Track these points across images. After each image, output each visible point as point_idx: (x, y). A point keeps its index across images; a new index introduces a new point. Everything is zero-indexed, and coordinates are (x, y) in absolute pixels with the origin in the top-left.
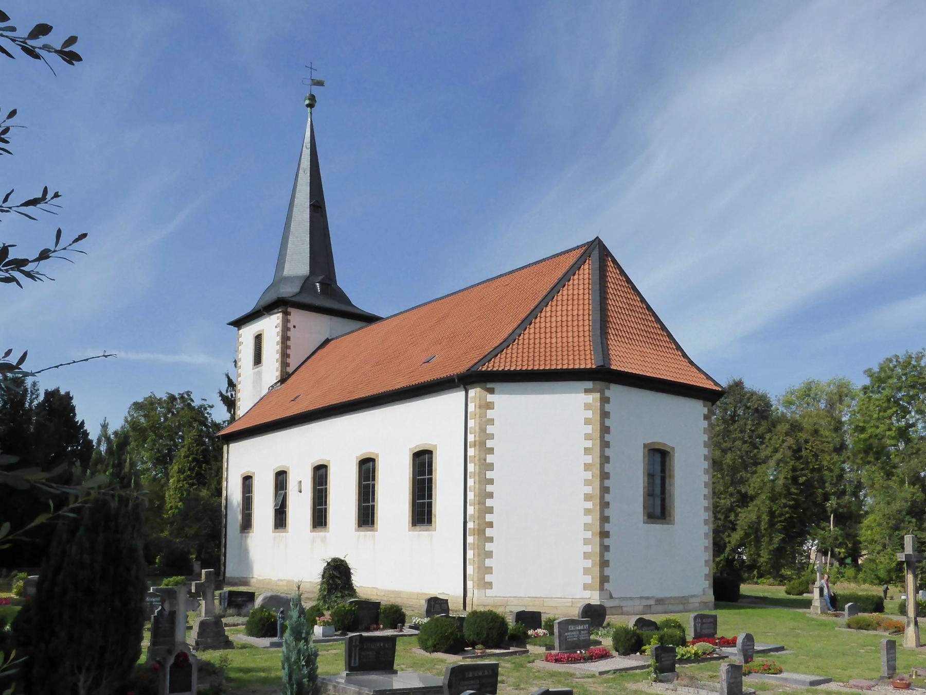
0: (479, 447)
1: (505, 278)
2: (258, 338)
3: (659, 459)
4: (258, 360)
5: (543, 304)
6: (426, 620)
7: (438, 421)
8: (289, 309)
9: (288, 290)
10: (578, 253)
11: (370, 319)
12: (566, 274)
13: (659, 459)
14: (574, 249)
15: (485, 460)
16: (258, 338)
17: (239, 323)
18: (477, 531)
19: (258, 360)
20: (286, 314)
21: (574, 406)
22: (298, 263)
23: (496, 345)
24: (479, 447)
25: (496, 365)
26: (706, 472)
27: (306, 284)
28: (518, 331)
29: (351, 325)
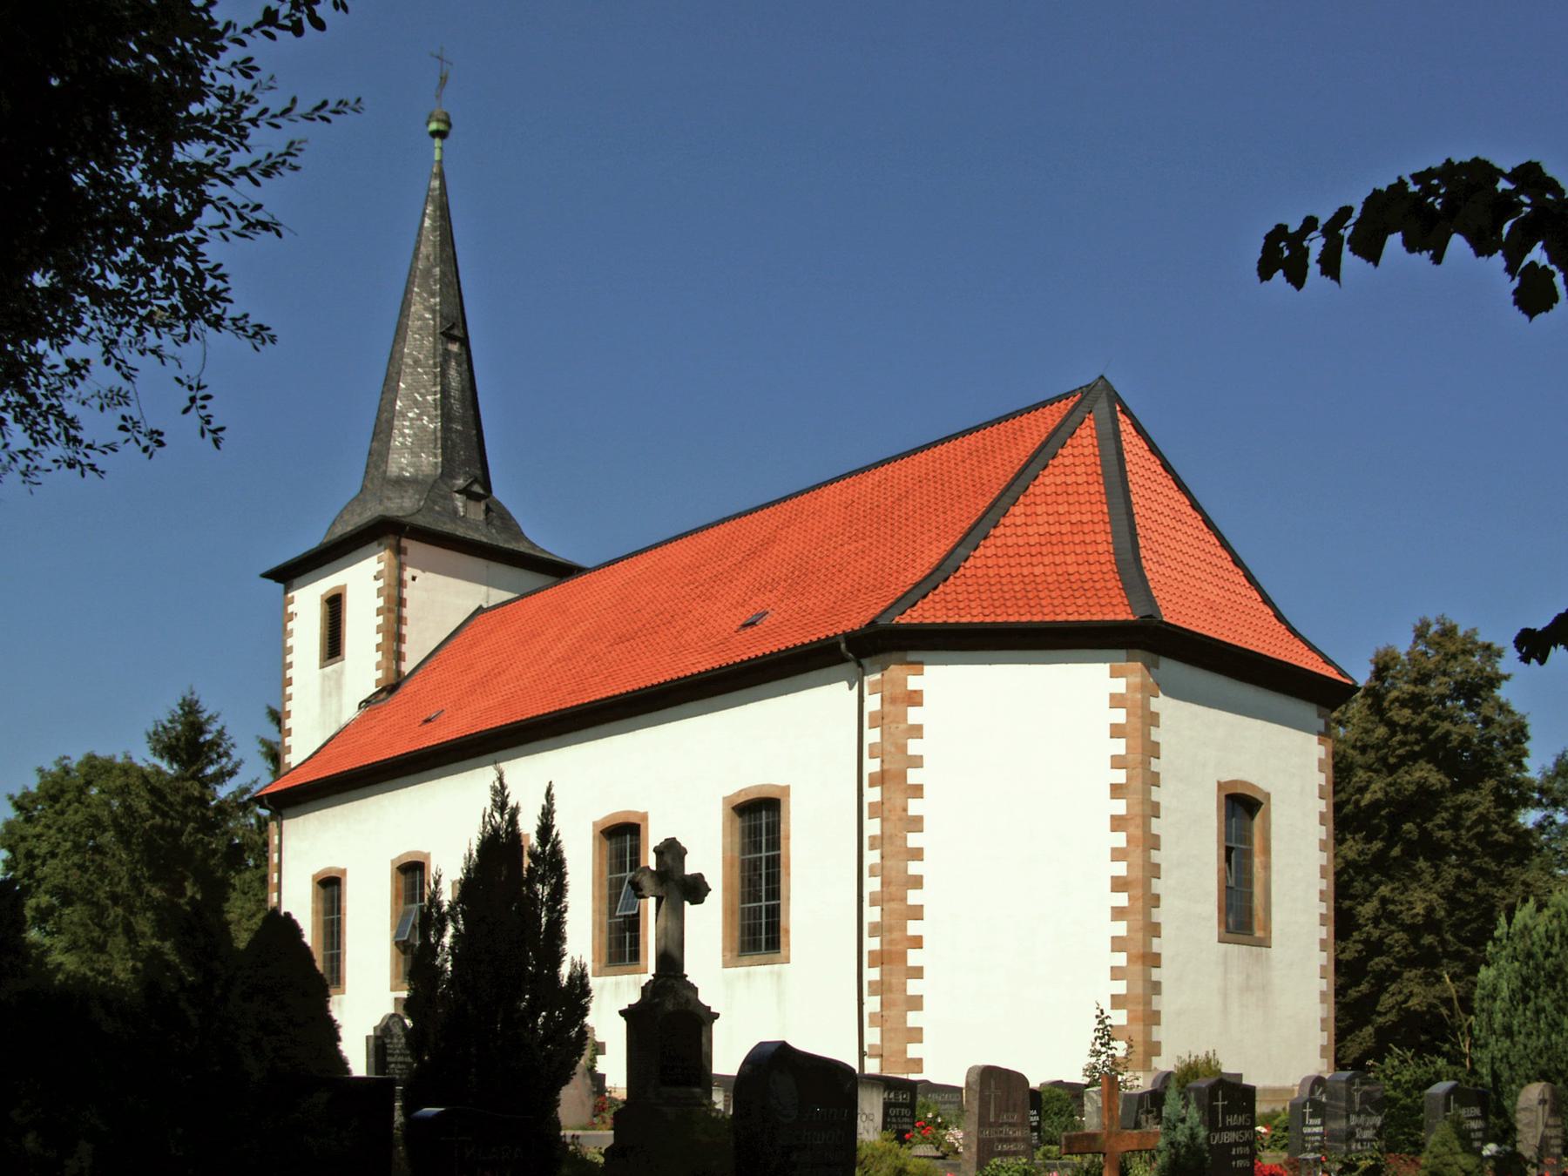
0: (889, 784)
1: (889, 468)
2: (334, 605)
3: (1242, 807)
4: (333, 647)
5: (1006, 500)
6: (1517, 279)
7: (800, 739)
8: (405, 542)
9: (401, 505)
10: (1064, 407)
11: (562, 571)
12: (1044, 445)
13: (1242, 807)
14: (1059, 399)
15: (905, 810)
16: (334, 605)
17: (290, 574)
18: (888, 959)
19: (333, 647)
20: (399, 551)
21: (1087, 689)
22: (412, 450)
23: (917, 579)
24: (889, 784)
25: (1135, 450)
26: (1323, 846)
27: (433, 488)
28: (961, 551)
29: (530, 579)
